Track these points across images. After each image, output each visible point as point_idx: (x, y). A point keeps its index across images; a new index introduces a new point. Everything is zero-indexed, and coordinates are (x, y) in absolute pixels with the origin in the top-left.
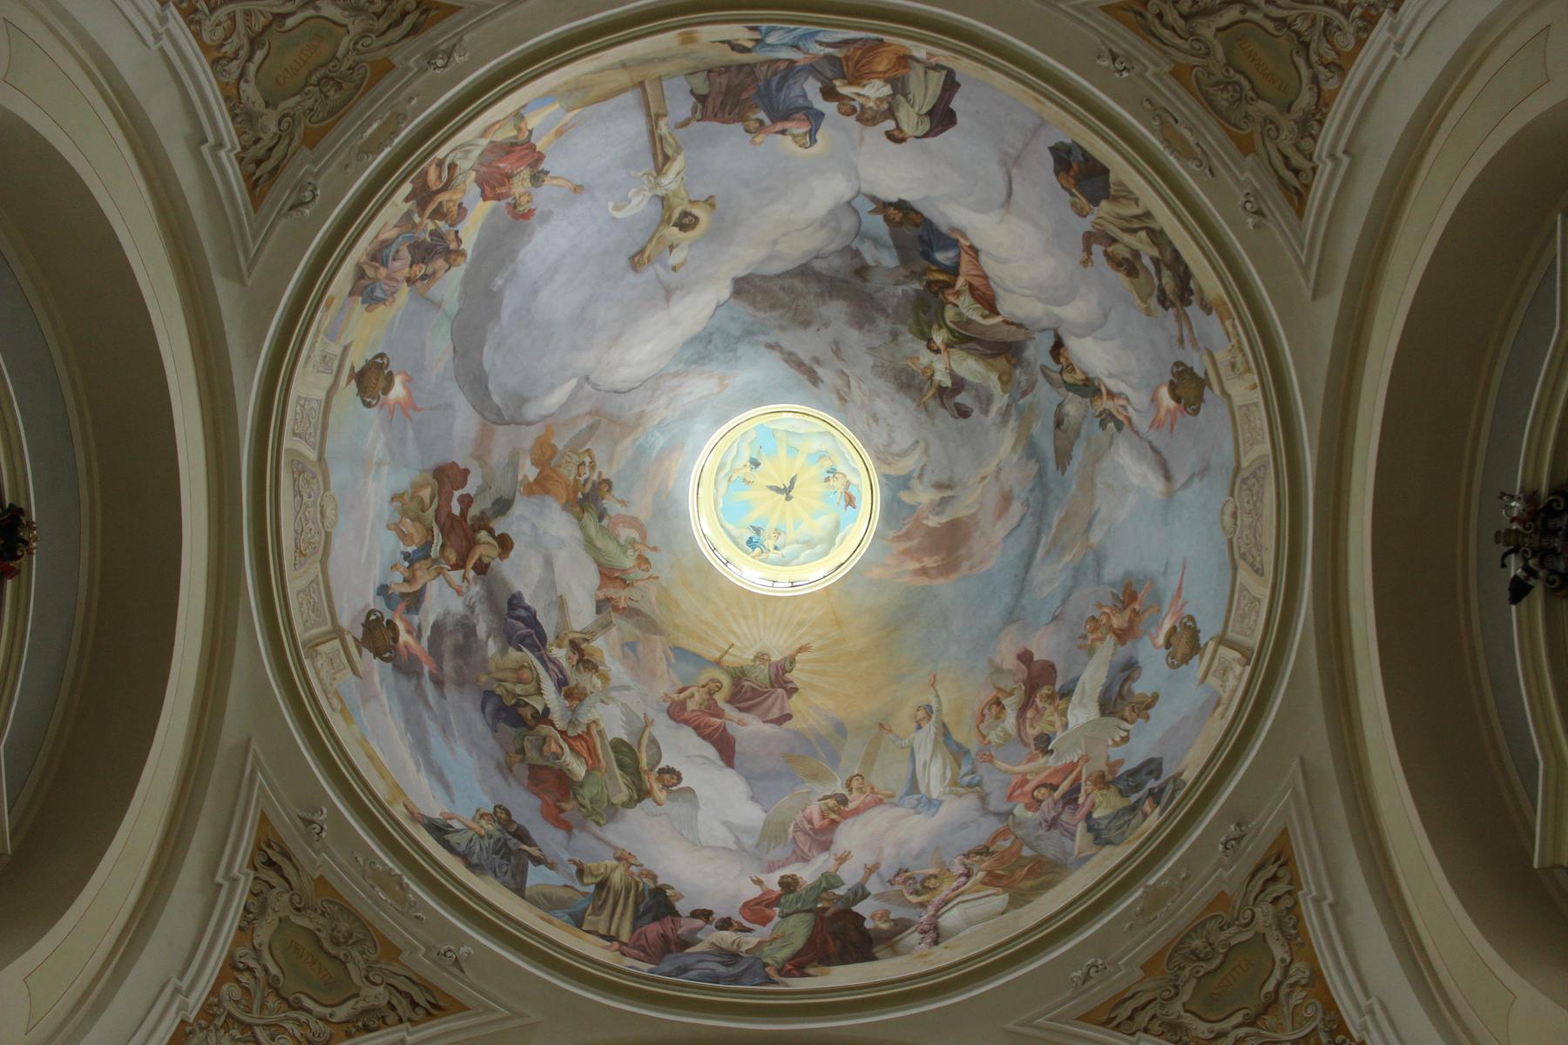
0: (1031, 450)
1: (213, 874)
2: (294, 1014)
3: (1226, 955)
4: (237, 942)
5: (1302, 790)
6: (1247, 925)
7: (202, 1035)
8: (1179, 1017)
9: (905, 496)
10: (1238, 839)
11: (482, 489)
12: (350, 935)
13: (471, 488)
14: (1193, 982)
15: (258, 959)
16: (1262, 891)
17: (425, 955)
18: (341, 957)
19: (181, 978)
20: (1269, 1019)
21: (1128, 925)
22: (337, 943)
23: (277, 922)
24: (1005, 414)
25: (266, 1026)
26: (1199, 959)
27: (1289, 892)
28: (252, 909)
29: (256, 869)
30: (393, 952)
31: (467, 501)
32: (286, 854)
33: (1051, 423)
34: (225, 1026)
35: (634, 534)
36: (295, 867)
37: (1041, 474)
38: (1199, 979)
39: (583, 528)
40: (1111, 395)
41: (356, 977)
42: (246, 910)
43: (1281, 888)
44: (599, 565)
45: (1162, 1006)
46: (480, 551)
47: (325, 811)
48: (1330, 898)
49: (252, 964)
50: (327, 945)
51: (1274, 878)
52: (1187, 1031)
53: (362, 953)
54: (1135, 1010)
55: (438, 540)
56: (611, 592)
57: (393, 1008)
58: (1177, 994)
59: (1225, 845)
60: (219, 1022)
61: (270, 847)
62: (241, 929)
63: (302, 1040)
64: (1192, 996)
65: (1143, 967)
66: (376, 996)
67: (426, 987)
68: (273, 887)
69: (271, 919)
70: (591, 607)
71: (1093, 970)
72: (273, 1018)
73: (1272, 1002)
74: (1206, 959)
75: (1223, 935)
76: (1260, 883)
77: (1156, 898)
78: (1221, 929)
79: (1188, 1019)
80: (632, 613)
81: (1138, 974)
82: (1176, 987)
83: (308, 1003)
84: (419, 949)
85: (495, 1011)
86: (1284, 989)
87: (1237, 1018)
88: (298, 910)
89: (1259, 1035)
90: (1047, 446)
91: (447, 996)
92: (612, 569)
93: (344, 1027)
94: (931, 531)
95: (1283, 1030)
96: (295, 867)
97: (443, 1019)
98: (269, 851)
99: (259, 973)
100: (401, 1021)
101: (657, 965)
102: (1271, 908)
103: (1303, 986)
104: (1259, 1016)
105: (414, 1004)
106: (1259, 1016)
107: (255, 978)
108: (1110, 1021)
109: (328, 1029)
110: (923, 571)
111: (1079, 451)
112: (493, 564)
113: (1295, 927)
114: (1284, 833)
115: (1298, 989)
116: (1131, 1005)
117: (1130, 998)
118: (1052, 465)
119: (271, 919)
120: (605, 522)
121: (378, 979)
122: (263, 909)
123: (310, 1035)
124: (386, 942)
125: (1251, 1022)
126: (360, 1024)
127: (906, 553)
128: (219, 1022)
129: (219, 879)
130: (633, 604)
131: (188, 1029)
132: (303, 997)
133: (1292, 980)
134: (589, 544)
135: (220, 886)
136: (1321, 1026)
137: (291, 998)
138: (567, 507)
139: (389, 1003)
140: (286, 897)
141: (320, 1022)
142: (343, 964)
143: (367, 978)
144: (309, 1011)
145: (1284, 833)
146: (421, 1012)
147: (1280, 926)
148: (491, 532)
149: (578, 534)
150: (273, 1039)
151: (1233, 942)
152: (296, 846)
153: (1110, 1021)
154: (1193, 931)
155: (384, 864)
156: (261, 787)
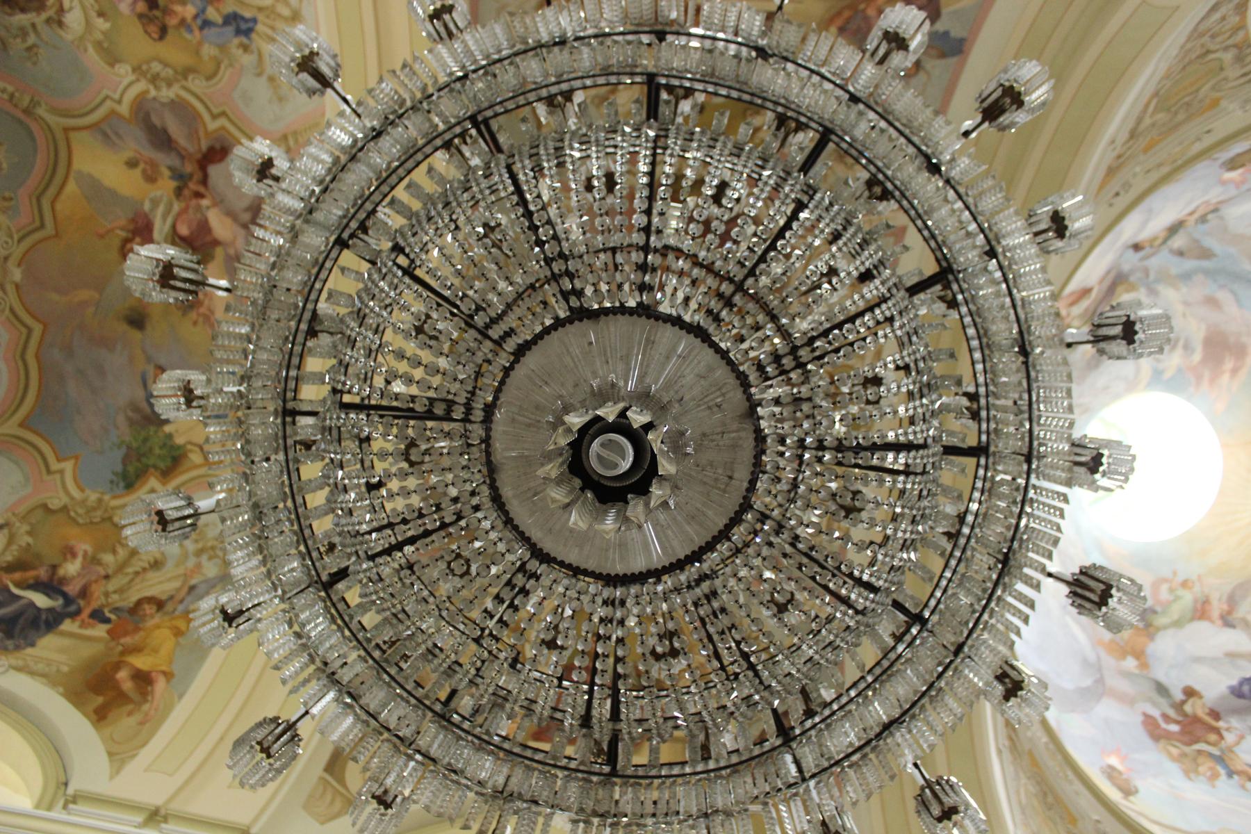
0: (1186, 277)
9: (1168, 375)
11: (1154, 704)
13: (1155, 713)
24: (1152, 292)
31: (1166, 718)
33: (1176, 259)
35: (1165, 587)
37: (1207, 273)
39: (1165, 627)
40: (1191, 214)
44: (1193, 619)
46: (1201, 713)
55: (1201, 746)
56: (1215, 613)
70: (1229, 631)
80: (1232, 601)
90: (1189, 264)
92: (1195, 610)
94: (1204, 361)
110: (1235, 371)
111: (1209, 242)
112: (1209, 704)
118: (1206, 264)
120: (1158, 609)
127: (1213, 380)
130: (1225, 598)
134: (1178, 624)
138: (1151, 637)
148: (1183, 702)
149: (1170, 632)
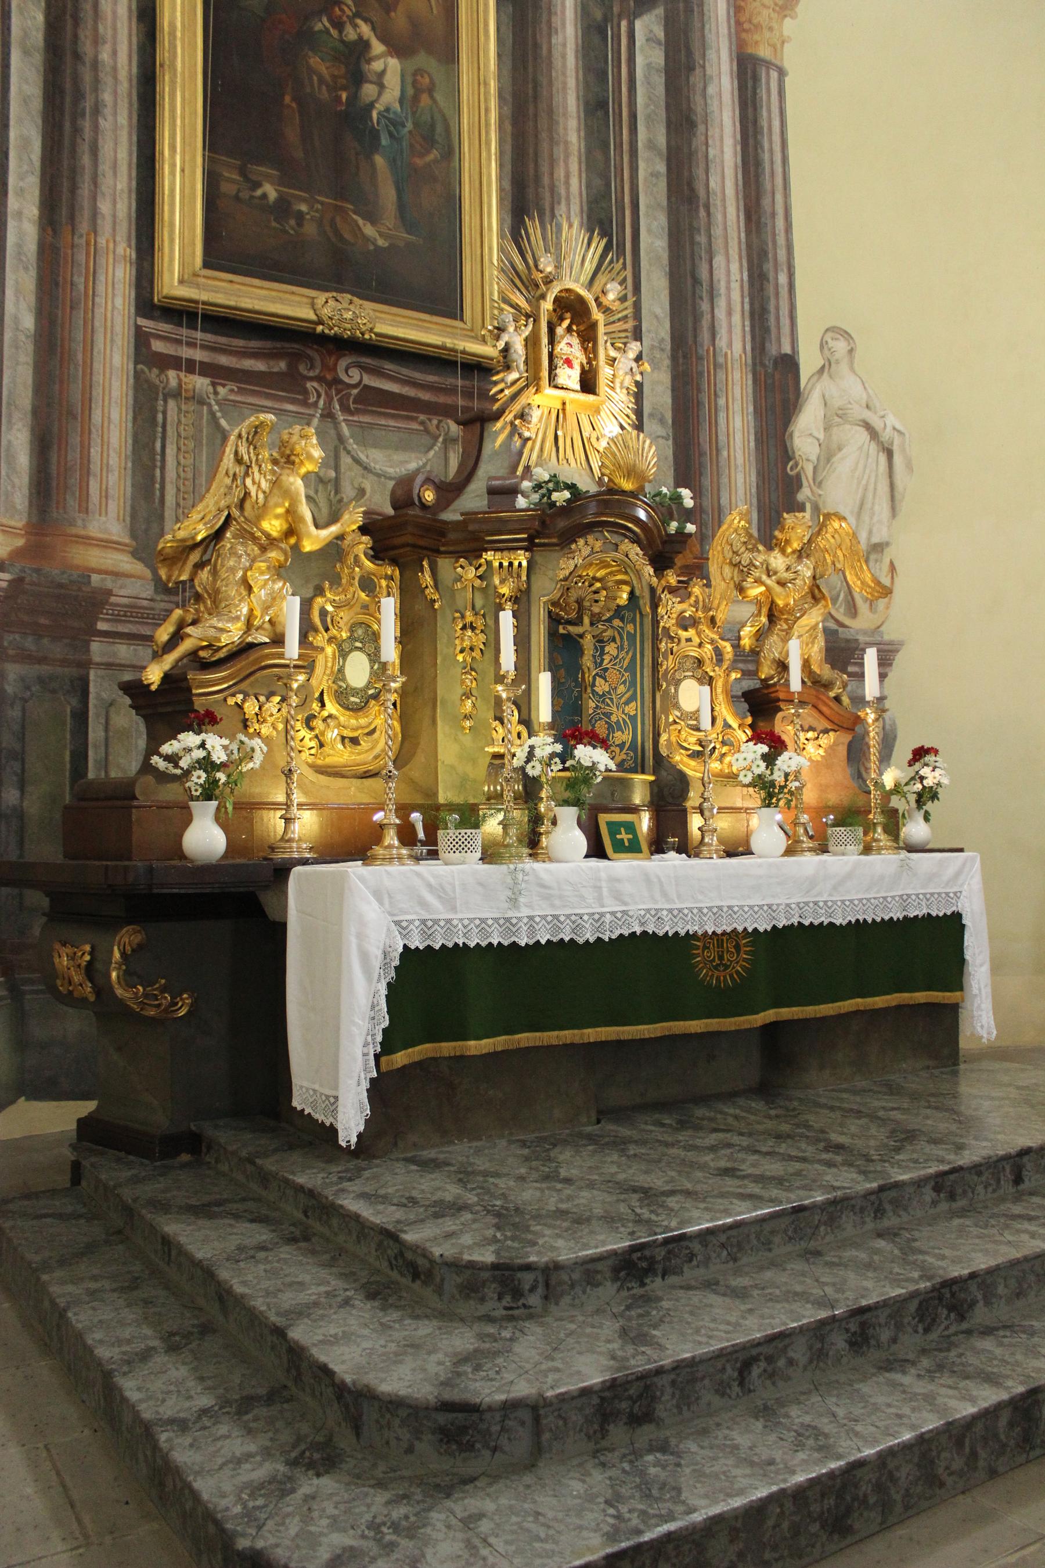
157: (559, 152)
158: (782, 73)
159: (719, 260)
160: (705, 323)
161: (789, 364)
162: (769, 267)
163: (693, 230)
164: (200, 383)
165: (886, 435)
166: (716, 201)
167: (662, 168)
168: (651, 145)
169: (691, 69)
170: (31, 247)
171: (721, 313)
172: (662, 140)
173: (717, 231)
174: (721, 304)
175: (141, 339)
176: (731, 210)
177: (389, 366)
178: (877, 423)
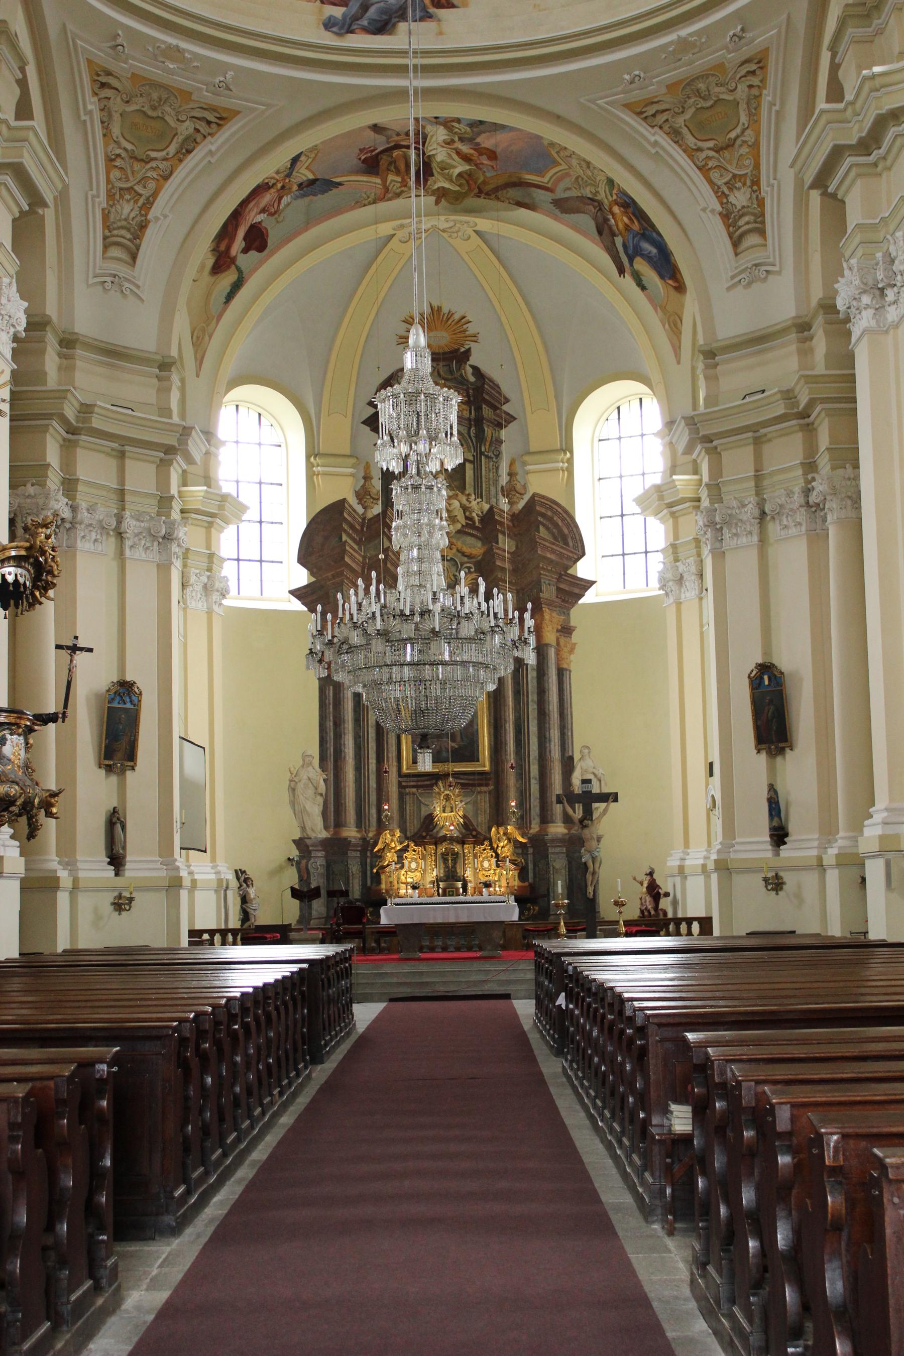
1: (79, 117)
2: (149, 166)
3: (716, 102)
4: (106, 145)
5: (783, 34)
6: (732, 91)
7: (113, 210)
8: (680, 127)
10: (740, 38)
12: (160, 99)
14: (693, 109)
15: (120, 147)
16: (745, 76)
17: (207, 91)
18: (160, 115)
19: (92, 190)
20: (726, 154)
21: (664, 56)
22: (154, 108)
23: (120, 118)
25: (140, 181)
26: (701, 97)
27: (759, 86)
28: (105, 119)
29: (97, 94)
30: (187, 95)
32: (109, 73)
34: (121, 196)
36: (116, 77)
38: (697, 109)
41: (172, 123)
42: (102, 122)
43: (755, 81)
45: (673, 117)
47: (120, 33)
48: (777, 108)
49: (118, 151)
50: (150, 113)
51: (753, 73)
52: (683, 138)
53: (170, 106)
54: (657, 112)
57: (197, 130)
58: (683, 112)
59: (731, 38)
60: (117, 197)
61: (98, 75)
62: (104, 135)
63: (158, 178)
64: (691, 117)
65: (667, 86)
66: (186, 128)
67: (212, 109)
68: (109, 99)
69: (116, 117)
71: (637, 78)
72: (139, 176)
73: (730, 145)
74: (704, 99)
75: (717, 89)
76: (745, 71)
77: (684, 45)
78: (717, 84)
79: (685, 131)
81: (664, 90)
82: (683, 108)
83: (153, 154)
84: (201, 89)
85: (256, 109)
86: (738, 142)
87: (711, 144)
88: (127, 102)
89: (720, 161)
91: (226, 109)
93: (176, 157)
95: (731, 164)
96: (116, 77)
97: (228, 125)
98: (100, 79)
99: (124, 154)
100: (205, 137)
101: (346, 5)
102: (747, 89)
103: (749, 146)
104: (722, 149)
105: (209, 123)
106: (722, 149)
107: (123, 158)
108: (641, 113)
109: (169, 163)
113: (755, 109)
114: (767, 49)
115: (745, 146)
116: (655, 108)
117: (656, 103)
119: (116, 117)
121: (184, 118)
122: (110, 115)
123: (161, 173)
124: (181, 91)
125: (718, 149)
126: (184, 151)
128: (117, 197)
129: (83, 118)
131: (106, 212)
132: (149, 153)
133: (744, 139)
135: (85, 121)
136: (749, 174)
137: (144, 157)
139: (195, 129)
140: (119, 99)
141: (164, 162)
142: (163, 118)
143: (178, 120)
144: (155, 159)
145: (767, 49)
146: (214, 126)
147: (748, 104)
150: (145, 187)
151: (722, 97)
152: (112, 66)
153: (641, 113)
154: (703, 77)
155: (165, 42)
156: (81, 46)
157: (507, 708)
158: (570, 671)
159: (552, 731)
160: (548, 750)
161: (571, 758)
162: (566, 731)
163: (545, 723)
164: (414, 790)
165: (599, 775)
166: (551, 714)
167: (535, 706)
168: (533, 701)
169: (544, 675)
170: (374, 769)
171: (552, 746)
172: (536, 699)
173: (552, 722)
174: (552, 744)
175: (400, 783)
176: (556, 715)
177: (461, 776)
178: (597, 772)
